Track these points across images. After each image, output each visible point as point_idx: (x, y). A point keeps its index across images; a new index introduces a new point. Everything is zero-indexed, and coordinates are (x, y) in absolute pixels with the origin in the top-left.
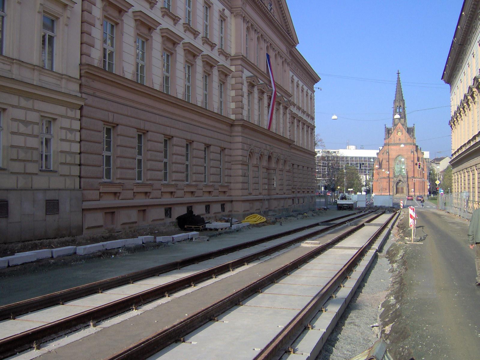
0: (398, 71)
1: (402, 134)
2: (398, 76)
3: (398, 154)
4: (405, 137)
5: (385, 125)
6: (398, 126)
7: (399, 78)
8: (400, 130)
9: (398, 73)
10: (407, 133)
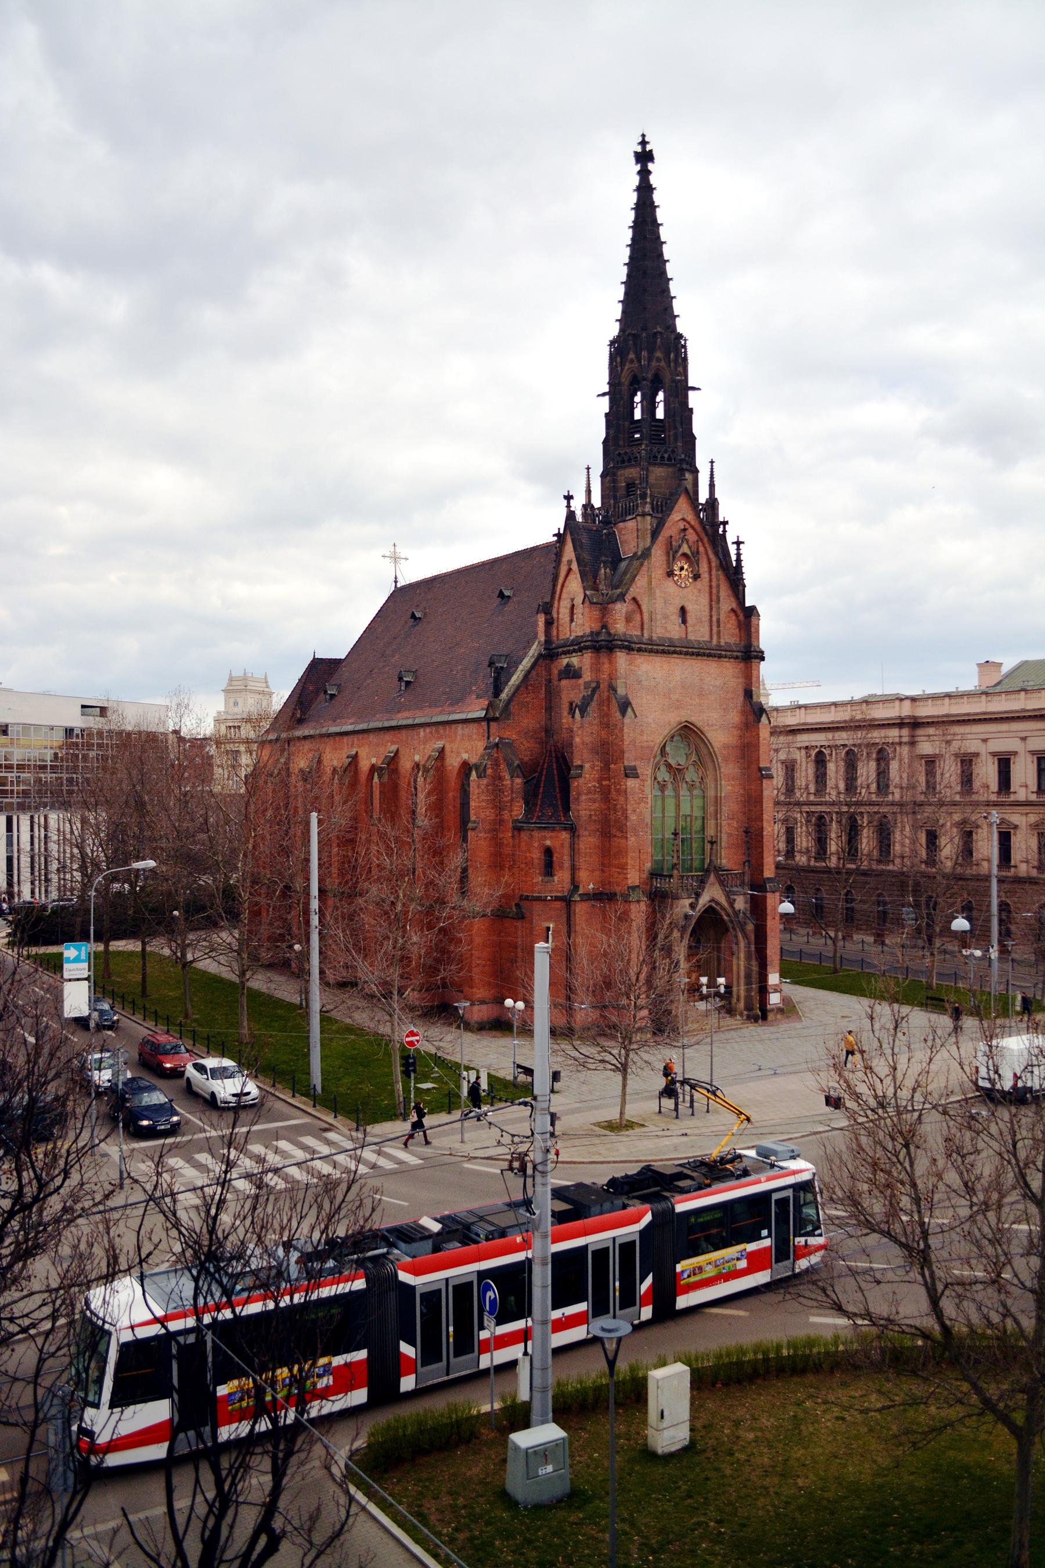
0: (644, 143)
1: (696, 577)
2: (644, 174)
3: (674, 719)
4: (714, 601)
5: (569, 498)
6: (675, 517)
7: (645, 190)
8: (685, 549)
9: (644, 157)
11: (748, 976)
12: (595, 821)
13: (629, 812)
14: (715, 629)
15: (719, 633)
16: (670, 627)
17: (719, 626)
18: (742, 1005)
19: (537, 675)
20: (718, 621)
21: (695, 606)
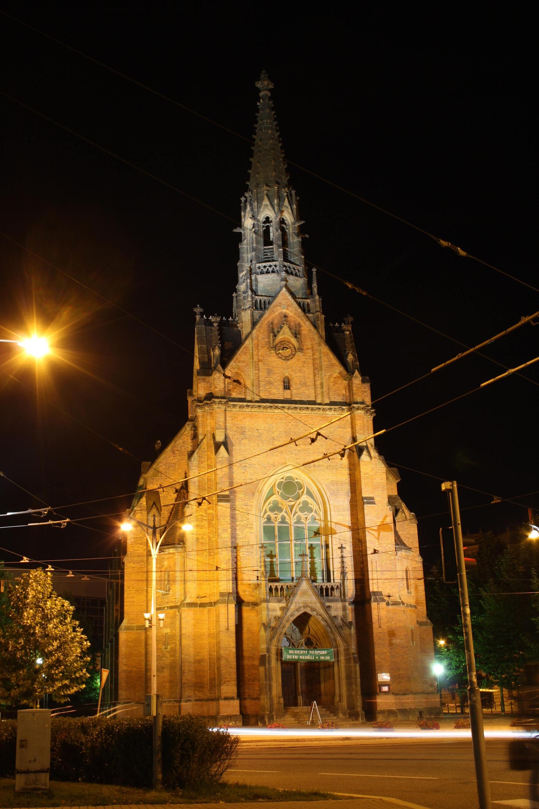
4: (317, 369)
10: (325, 349)
11: (349, 677)
12: (202, 543)
13: (220, 531)
14: (319, 391)
15: (322, 393)
16: (274, 391)
17: (322, 388)
18: (345, 703)
19: (184, 442)
20: (322, 384)
21: (300, 374)
